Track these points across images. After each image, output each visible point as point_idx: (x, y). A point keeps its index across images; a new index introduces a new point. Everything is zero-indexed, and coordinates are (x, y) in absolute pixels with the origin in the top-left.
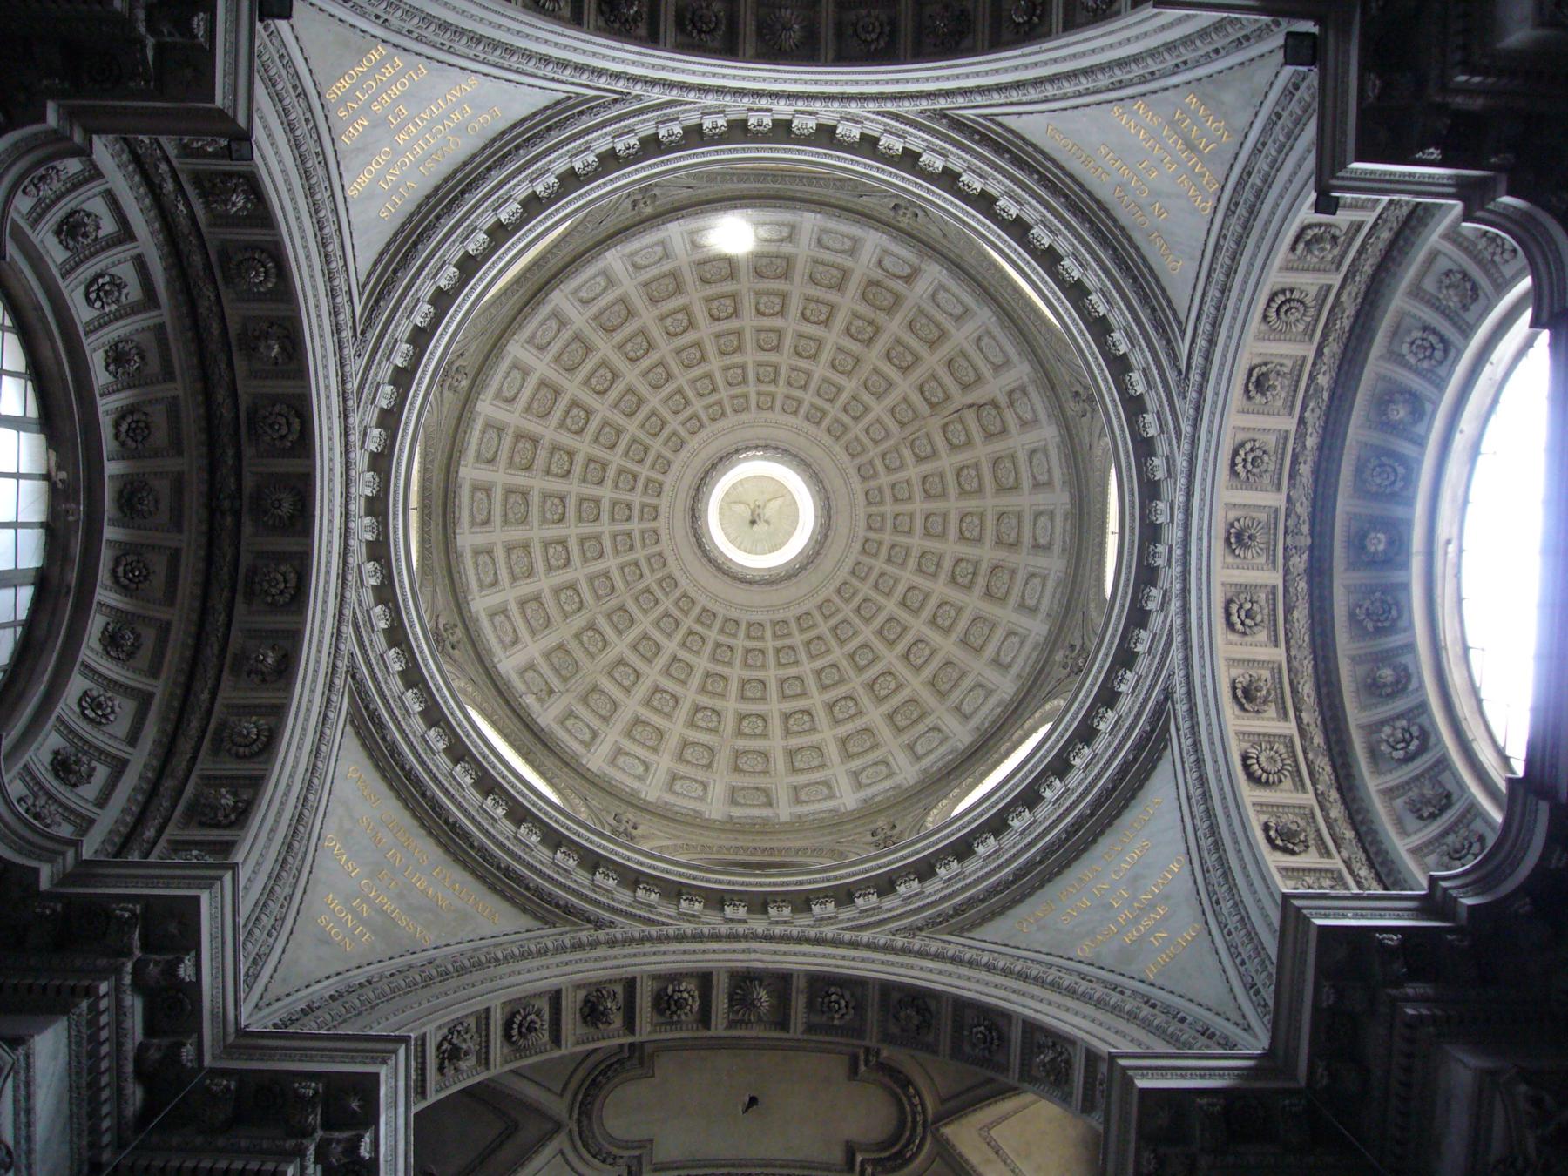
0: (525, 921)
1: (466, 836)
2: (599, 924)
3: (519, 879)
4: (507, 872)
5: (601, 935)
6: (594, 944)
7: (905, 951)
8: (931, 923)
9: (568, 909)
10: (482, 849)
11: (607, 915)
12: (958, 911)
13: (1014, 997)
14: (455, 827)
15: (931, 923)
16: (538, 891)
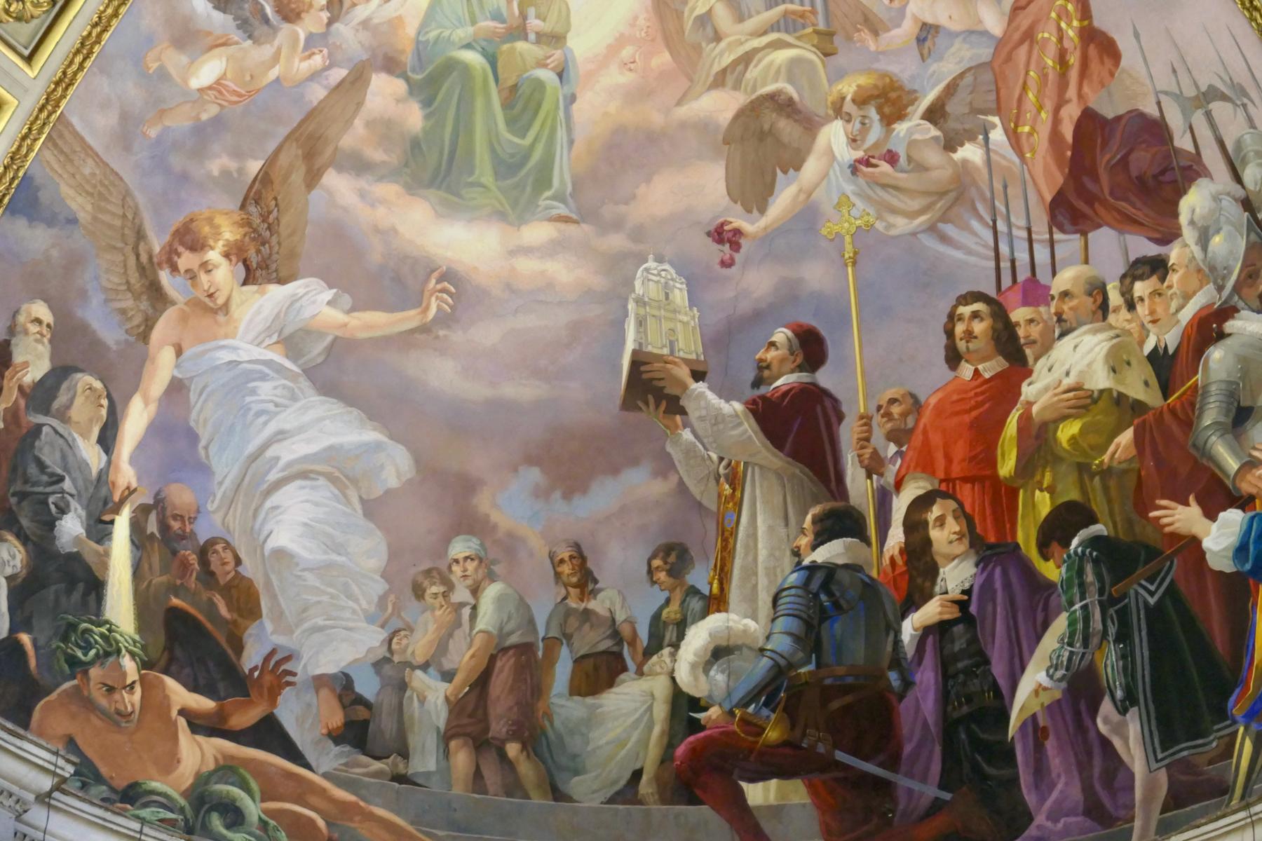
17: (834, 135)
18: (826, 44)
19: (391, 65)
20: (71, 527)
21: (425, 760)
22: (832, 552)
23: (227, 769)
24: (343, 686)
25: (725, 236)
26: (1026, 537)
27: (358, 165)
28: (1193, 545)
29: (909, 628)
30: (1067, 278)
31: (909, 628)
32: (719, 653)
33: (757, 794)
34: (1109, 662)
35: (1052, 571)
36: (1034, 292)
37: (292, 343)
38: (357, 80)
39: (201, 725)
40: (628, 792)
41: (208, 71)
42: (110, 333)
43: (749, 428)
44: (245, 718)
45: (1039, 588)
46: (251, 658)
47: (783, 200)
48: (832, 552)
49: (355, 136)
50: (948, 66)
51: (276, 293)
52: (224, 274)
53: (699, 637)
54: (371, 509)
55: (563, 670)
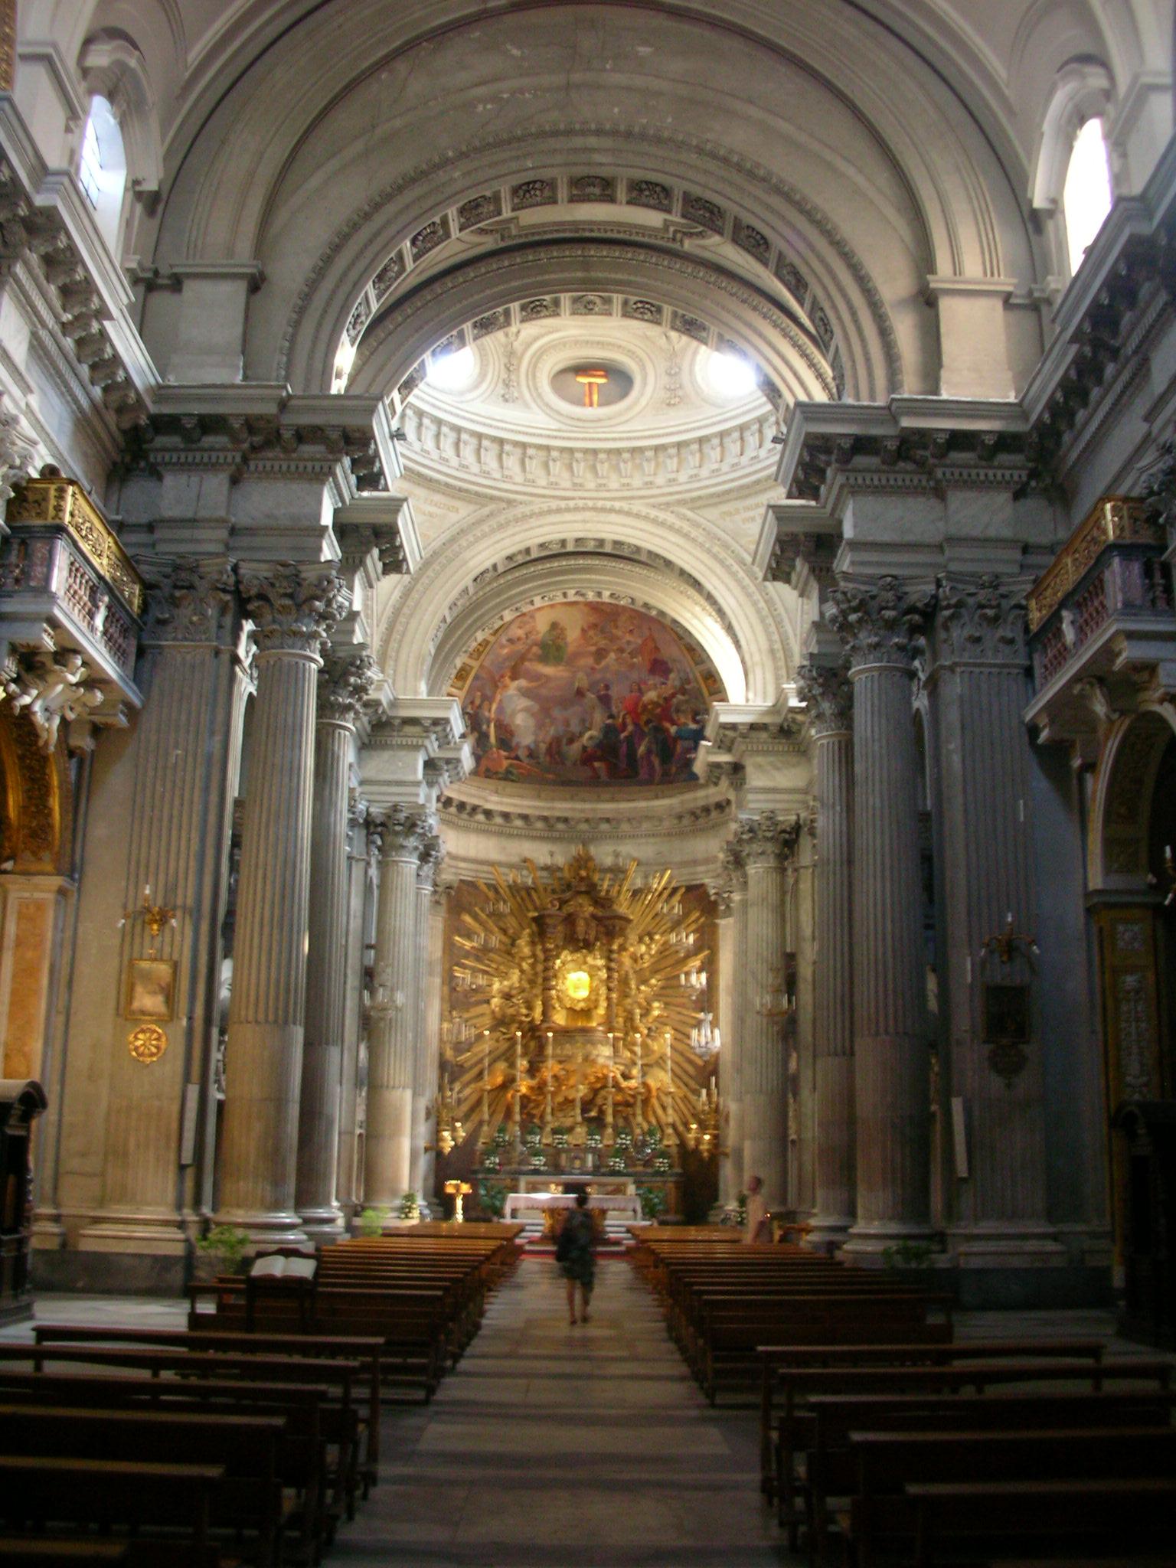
0: (472, 507)
1: (437, 481)
2: (510, 503)
3: (467, 491)
4: (460, 490)
5: (511, 513)
6: (508, 523)
7: (663, 524)
8: (680, 503)
9: (492, 498)
10: (447, 485)
11: (512, 496)
12: (693, 500)
13: (708, 573)
14: (431, 480)
15: (682, 503)
16: (477, 494)
17: (612, 655)
18: (611, 641)
19: (536, 644)
20: (484, 727)
21: (542, 759)
22: (610, 721)
23: (511, 765)
24: (528, 747)
25: (593, 669)
26: (642, 723)
27: (530, 660)
28: (667, 731)
29: (623, 736)
30: (651, 682)
31: (623, 736)
32: (591, 738)
33: (597, 764)
34: (654, 747)
35: (646, 729)
36: (645, 683)
37: (519, 689)
38: (531, 647)
39: (507, 758)
40: (574, 764)
41: (505, 651)
42: (489, 693)
43: (596, 701)
44: (513, 755)
45: (643, 731)
46: (514, 744)
47: (603, 663)
48: (610, 721)
49: (530, 656)
50: (632, 647)
51: (516, 683)
52: (507, 680)
53: (587, 735)
54: (533, 715)
55: (564, 741)
